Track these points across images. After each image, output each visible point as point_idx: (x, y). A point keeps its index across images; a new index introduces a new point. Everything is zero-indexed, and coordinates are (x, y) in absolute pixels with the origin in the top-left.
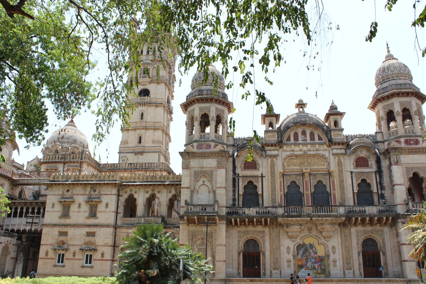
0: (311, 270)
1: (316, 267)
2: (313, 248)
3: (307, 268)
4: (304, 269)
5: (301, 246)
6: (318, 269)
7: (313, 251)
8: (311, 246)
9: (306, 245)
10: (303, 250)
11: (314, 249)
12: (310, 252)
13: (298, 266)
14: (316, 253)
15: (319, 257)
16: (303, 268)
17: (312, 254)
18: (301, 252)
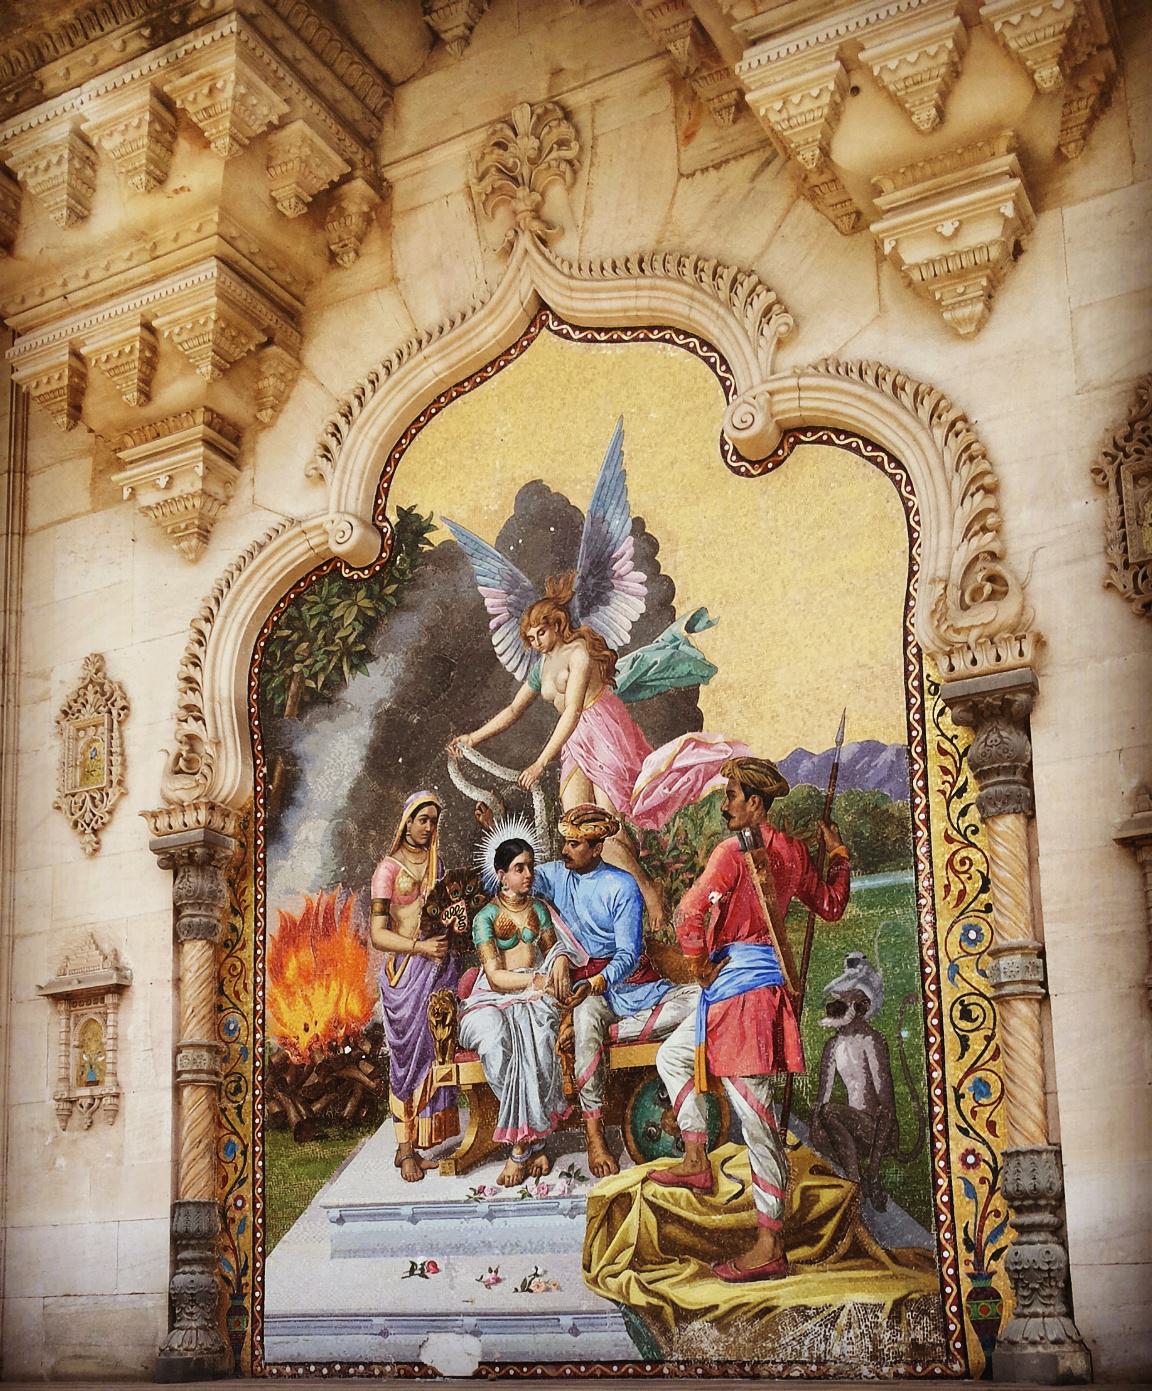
0: (541, 1152)
1: (672, 1062)
2: (599, 588)
3: (465, 1129)
4: (389, 1136)
5: (347, 615)
6: (722, 1126)
7: (603, 662)
8: (567, 555)
9: (451, 557)
10: (372, 688)
11: (622, 613)
12: (539, 717)
13: (281, 1075)
14: (671, 710)
15: (759, 782)
16: (371, 1116)
17: (590, 754)
18: (336, 756)
